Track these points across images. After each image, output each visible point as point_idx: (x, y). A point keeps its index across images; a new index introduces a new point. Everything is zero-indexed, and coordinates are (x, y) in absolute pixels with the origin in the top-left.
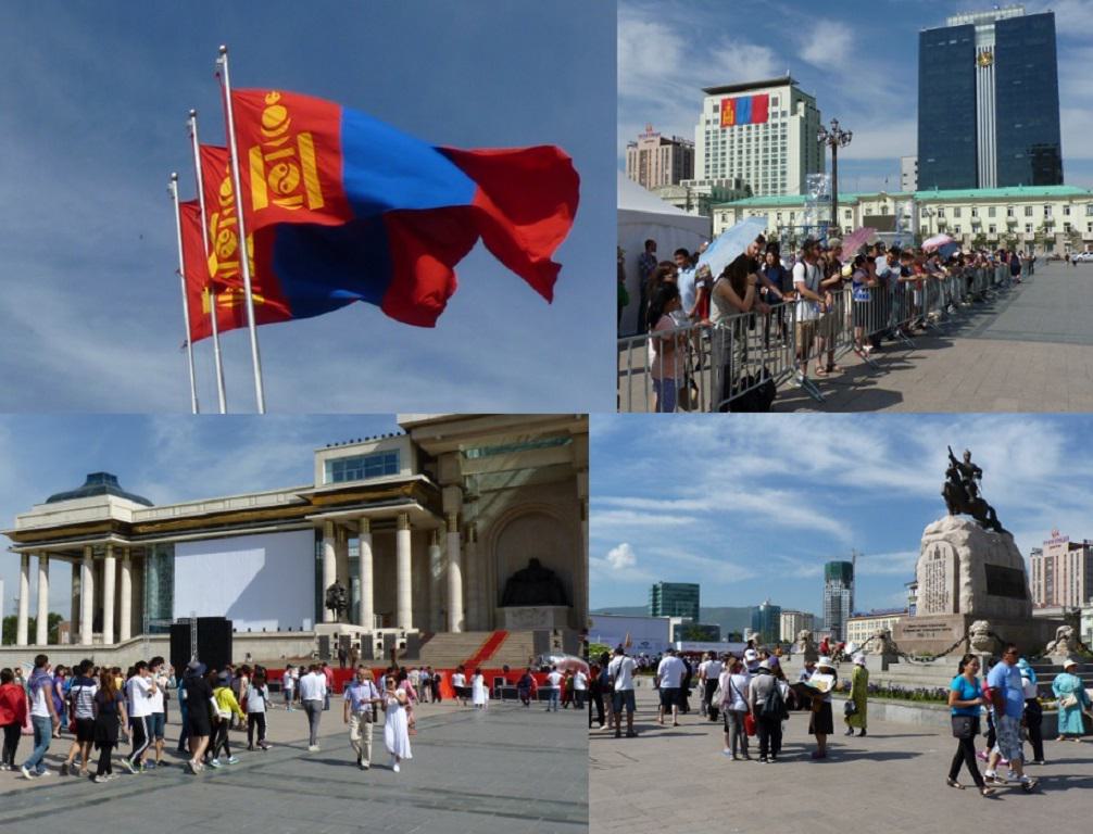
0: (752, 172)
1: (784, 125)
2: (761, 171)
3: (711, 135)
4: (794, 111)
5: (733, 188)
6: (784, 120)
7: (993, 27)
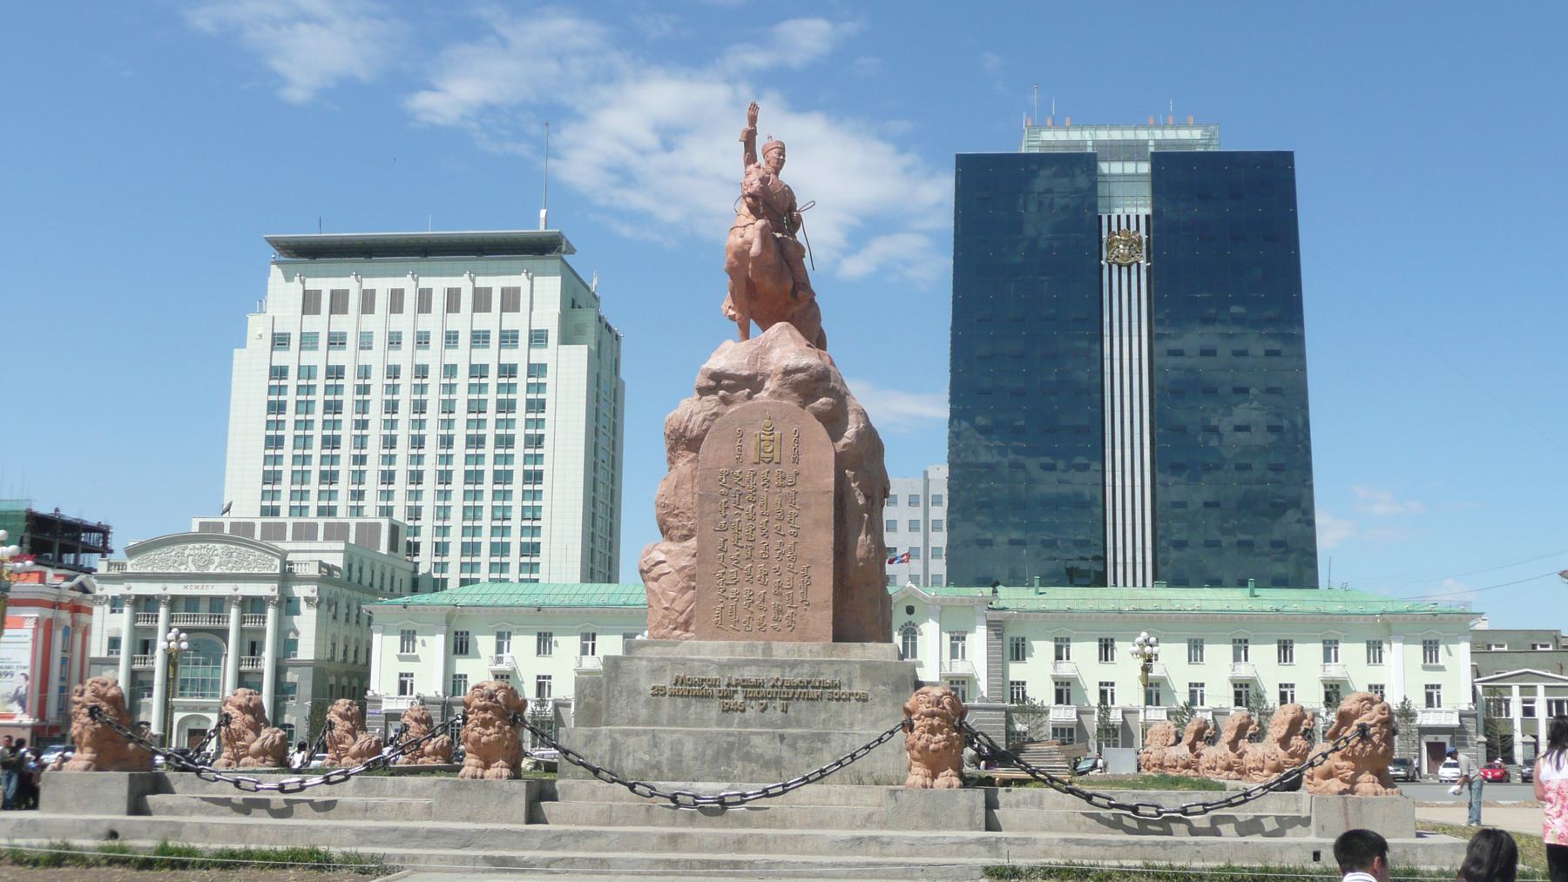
0: (428, 503)
1: (536, 370)
2: (457, 503)
3: (292, 381)
4: (569, 336)
5: (384, 548)
6: (538, 356)
7: (1145, 168)
